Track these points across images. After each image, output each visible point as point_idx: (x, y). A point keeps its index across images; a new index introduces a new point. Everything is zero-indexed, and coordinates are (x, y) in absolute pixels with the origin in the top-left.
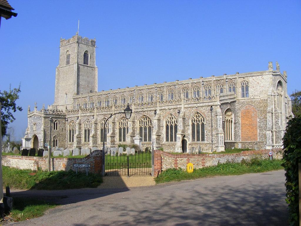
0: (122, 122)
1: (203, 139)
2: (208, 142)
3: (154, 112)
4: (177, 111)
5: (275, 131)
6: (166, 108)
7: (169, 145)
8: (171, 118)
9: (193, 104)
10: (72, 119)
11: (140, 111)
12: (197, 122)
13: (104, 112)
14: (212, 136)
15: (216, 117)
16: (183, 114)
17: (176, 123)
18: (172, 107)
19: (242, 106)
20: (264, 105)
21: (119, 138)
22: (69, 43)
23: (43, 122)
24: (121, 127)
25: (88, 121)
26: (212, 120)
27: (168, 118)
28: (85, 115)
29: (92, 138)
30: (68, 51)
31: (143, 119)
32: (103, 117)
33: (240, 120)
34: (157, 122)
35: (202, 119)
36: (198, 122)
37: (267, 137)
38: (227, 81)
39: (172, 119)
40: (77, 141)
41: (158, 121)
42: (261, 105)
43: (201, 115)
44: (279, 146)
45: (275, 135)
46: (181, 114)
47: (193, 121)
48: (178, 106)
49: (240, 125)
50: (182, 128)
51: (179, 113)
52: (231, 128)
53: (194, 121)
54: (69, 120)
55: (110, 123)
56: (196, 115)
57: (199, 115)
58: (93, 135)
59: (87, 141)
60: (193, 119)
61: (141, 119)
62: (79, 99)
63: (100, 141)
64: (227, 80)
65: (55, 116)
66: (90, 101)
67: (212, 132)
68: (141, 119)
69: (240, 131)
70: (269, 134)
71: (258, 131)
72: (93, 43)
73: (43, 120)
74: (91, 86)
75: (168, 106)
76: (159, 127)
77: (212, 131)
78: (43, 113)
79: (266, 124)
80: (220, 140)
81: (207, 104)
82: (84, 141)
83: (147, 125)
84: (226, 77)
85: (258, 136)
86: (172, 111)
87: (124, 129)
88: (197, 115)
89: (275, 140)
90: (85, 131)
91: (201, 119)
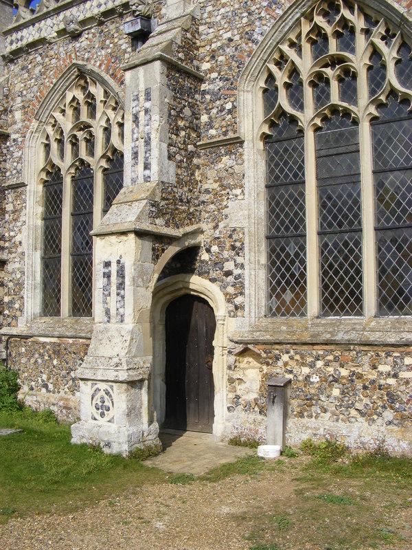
7: (57, 351)
56: (317, 29)
60: (281, 77)
88: (329, 29)
91: (376, 54)
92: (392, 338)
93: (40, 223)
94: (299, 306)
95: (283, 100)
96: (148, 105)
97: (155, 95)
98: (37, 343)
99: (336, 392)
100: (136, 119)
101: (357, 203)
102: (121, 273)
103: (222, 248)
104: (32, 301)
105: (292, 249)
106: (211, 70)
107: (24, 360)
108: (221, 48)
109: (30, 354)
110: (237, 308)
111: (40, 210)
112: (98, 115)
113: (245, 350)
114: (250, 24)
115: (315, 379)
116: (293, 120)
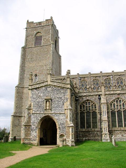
22: (40, 26)
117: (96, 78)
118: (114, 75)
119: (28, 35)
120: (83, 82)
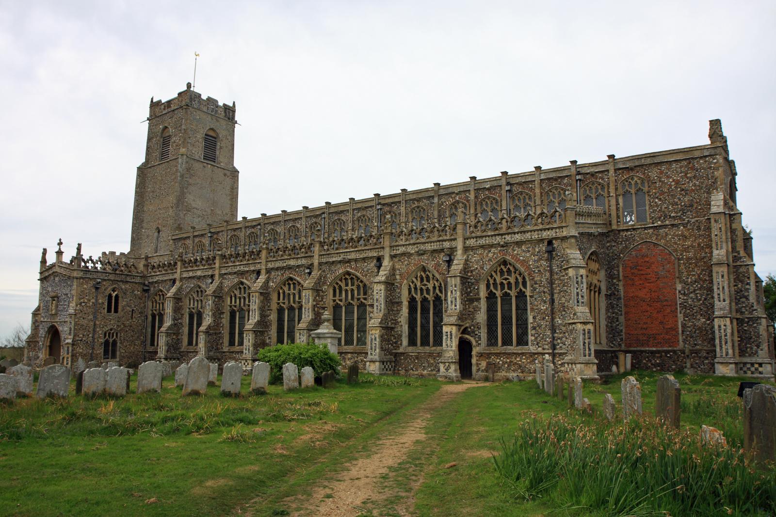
0: (287, 292)
1: (522, 341)
2: (540, 350)
3: (375, 261)
4: (443, 257)
5: (737, 319)
6: (409, 250)
8: (425, 279)
9: (492, 236)
10: (158, 286)
11: (334, 259)
12: (503, 288)
13: (238, 267)
14: (553, 330)
15: (567, 274)
16: (461, 267)
17: (437, 291)
18: (429, 247)
19: (626, 247)
20: (699, 244)
21: (276, 335)
23: (74, 292)
24: (282, 305)
25: (198, 291)
26: (551, 283)
27: (414, 280)
28: (191, 274)
29: (204, 336)
30: (166, 127)
31: (343, 285)
32: (236, 280)
33: (621, 288)
34: (383, 291)
35: (520, 280)
36: (506, 290)
37: (717, 336)
38: (580, 180)
39: (428, 281)
40: (167, 344)
41: (386, 290)
42: (688, 243)
43: (516, 270)
44: (752, 364)
45: (738, 331)
46: (457, 265)
47: (492, 285)
48: (447, 245)
49: (622, 301)
50: (458, 307)
51: (449, 262)
52: (595, 308)
53: (495, 284)
54: (152, 289)
55: (254, 294)
56: (502, 269)
57: (511, 268)
58: (209, 327)
59: (194, 342)
60: (491, 282)
61: (340, 283)
62: (188, 242)
63: (227, 344)
64: (578, 177)
65: (112, 277)
66: (212, 245)
67: (553, 319)
68: (337, 284)
69: (622, 319)
70: (723, 327)
71: (680, 317)
72: (229, 113)
73: (75, 287)
74: (220, 212)
75: (414, 244)
76: (392, 303)
77: (553, 313)
78: (75, 267)
79: (705, 299)
80: (582, 344)
81: (535, 236)
82: (186, 343)
83: (356, 300)
84: (578, 170)
85: (680, 332)
86: (428, 260)
87: (291, 309)
88: (505, 270)
89: (739, 345)
90: (191, 316)
91: (517, 279)
92: (520, 352)
93: (407, 315)
94: (496, 344)
95: (492, 288)
96: (455, 289)
97: (458, 286)
98: (409, 355)
99: (506, 366)
100: (452, 292)
101: (511, 317)
102: (451, 335)
103: (474, 328)
104: (405, 342)
105: (494, 329)
106: (471, 276)
107: (402, 361)
108: (474, 270)
109: (405, 359)
110: (479, 344)
111: (407, 311)
112: (431, 282)
113: (481, 355)
114: (483, 265)
115: (501, 362)
116: (495, 294)
117: (236, 233)
118: (265, 224)
119: (151, 136)
120: (362, 220)
